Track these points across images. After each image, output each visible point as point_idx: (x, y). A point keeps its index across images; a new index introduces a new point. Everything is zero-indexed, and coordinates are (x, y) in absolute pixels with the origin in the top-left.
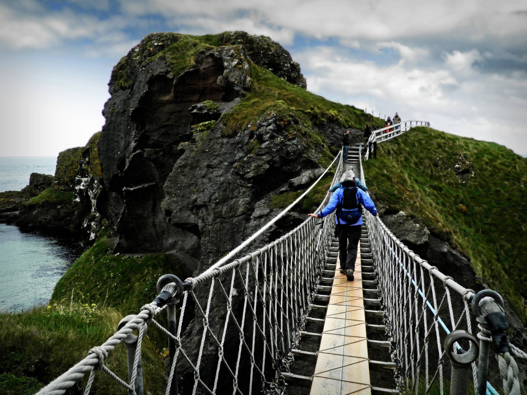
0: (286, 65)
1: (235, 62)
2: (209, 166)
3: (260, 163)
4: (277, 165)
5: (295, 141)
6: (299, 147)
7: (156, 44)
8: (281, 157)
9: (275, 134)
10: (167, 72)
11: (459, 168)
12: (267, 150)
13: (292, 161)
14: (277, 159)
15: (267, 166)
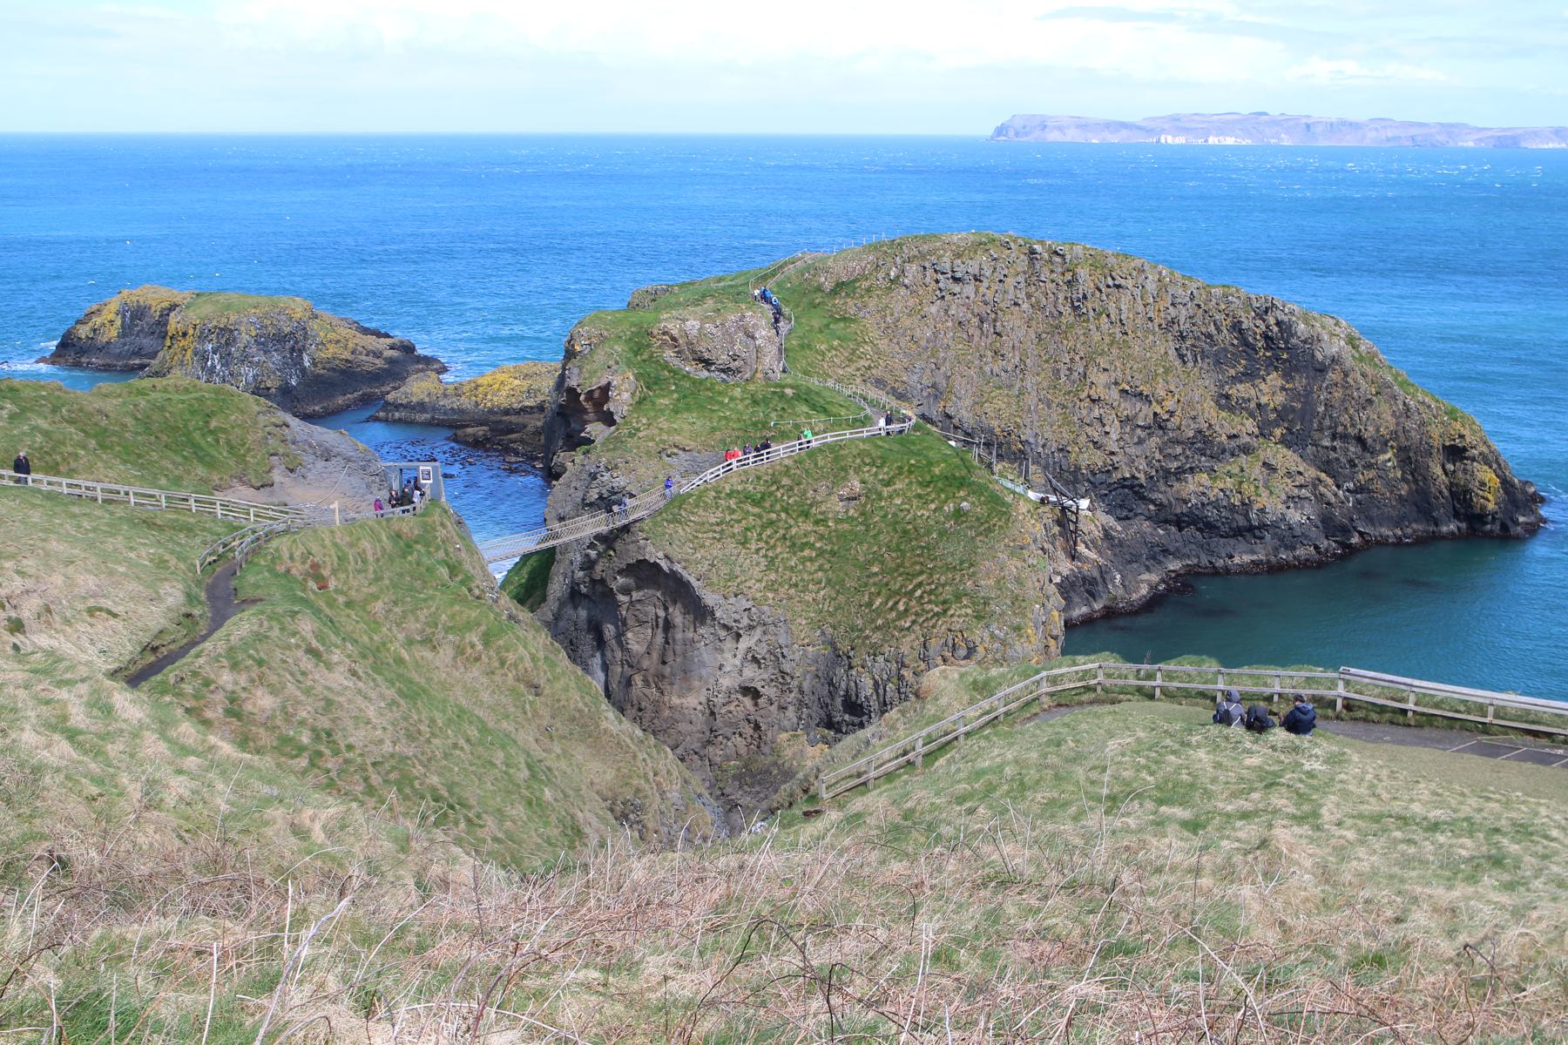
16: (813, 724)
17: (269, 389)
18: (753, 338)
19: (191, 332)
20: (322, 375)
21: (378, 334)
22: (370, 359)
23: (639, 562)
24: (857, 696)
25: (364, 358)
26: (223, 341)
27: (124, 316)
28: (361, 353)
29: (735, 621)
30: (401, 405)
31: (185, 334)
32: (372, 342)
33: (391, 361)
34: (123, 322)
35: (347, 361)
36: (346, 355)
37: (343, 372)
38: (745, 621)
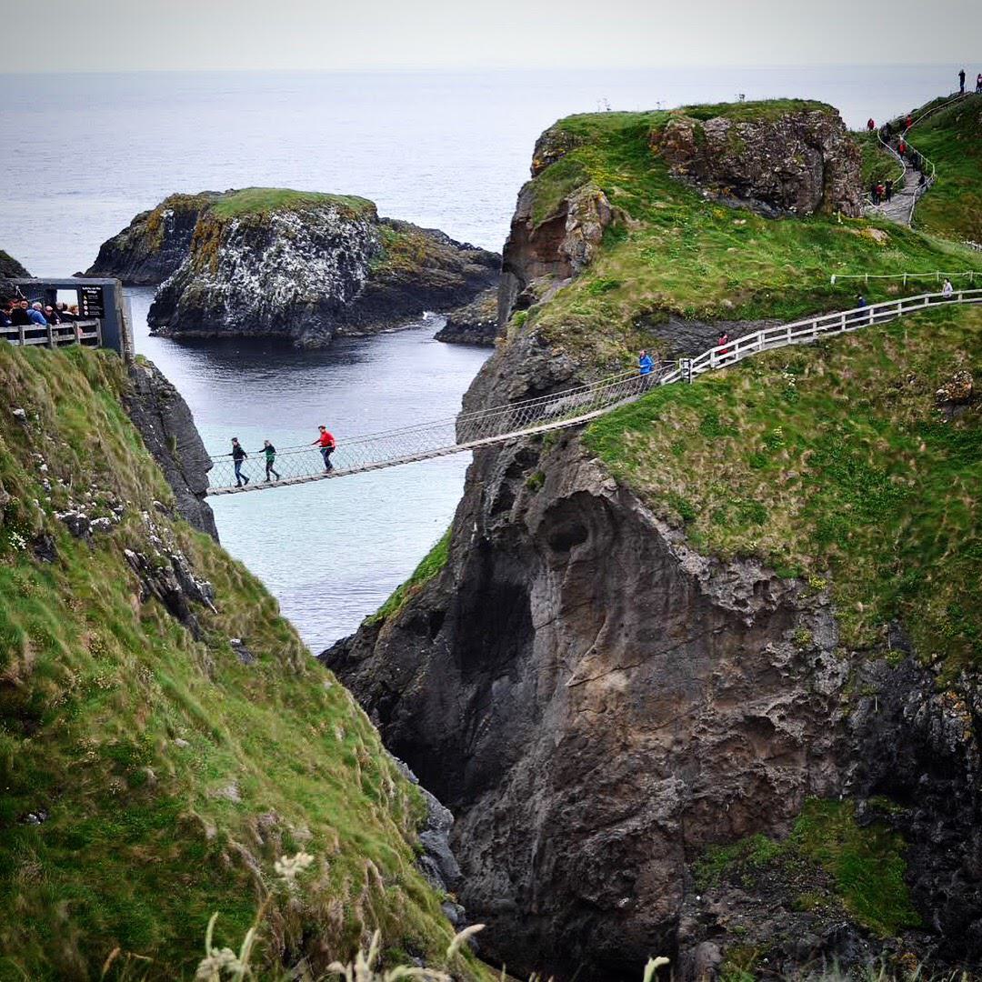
0: (764, 175)
1: (574, 225)
2: (502, 376)
3: (519, 383)
4: (538, 387)
5: (559, 360)
6: (565, 366)
7: (545, 153)
8: (542, 378)
9: (536, 349)
10: (528, 218)
11: (942, 396)
12: (526, 369)
13: (559, 382)
14: (536, 380)
15: (525, 388)
16: (866, 787)
17: (306, 303)
18: (819, 148)
19: (216, 232)
20: (379, 290)
21: (466, 246)
22: (445, 273)
23: (578, 494)
24: (941, 741)
25: (435, 271)
26: (253, 243)
27: (167, 224)
28: (433, 267)
29: (737, 602)
30: (466, 325)
31: (210, 235)
32: (448, 254)
33: (472, 277)
34: (166, 231)
35: (412, 273)
36: (414, 267)
37: (405, 287)
38: (754, 606)
